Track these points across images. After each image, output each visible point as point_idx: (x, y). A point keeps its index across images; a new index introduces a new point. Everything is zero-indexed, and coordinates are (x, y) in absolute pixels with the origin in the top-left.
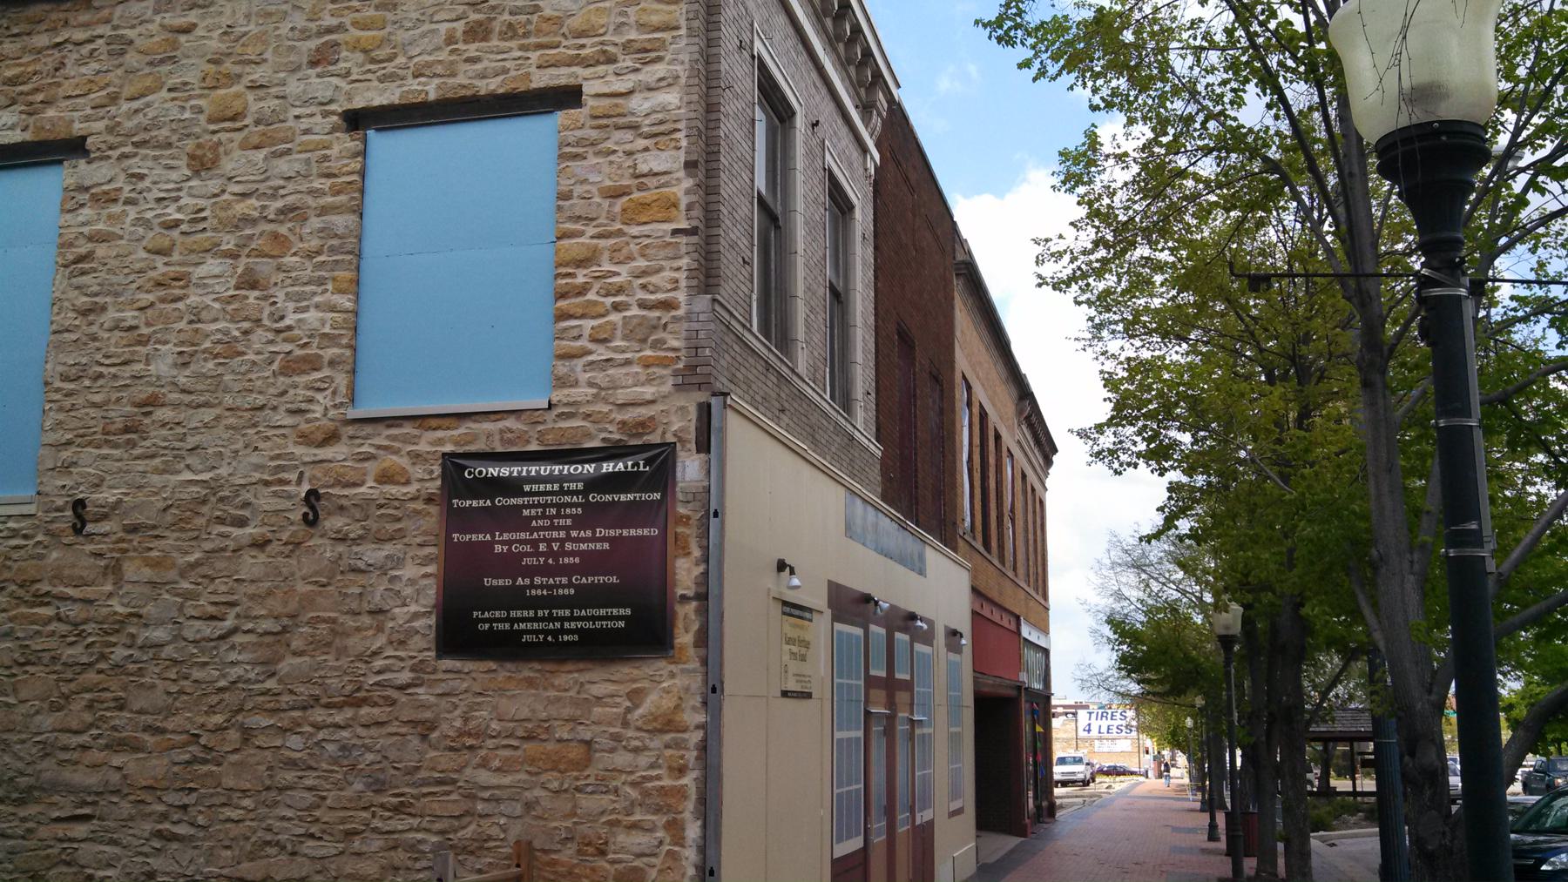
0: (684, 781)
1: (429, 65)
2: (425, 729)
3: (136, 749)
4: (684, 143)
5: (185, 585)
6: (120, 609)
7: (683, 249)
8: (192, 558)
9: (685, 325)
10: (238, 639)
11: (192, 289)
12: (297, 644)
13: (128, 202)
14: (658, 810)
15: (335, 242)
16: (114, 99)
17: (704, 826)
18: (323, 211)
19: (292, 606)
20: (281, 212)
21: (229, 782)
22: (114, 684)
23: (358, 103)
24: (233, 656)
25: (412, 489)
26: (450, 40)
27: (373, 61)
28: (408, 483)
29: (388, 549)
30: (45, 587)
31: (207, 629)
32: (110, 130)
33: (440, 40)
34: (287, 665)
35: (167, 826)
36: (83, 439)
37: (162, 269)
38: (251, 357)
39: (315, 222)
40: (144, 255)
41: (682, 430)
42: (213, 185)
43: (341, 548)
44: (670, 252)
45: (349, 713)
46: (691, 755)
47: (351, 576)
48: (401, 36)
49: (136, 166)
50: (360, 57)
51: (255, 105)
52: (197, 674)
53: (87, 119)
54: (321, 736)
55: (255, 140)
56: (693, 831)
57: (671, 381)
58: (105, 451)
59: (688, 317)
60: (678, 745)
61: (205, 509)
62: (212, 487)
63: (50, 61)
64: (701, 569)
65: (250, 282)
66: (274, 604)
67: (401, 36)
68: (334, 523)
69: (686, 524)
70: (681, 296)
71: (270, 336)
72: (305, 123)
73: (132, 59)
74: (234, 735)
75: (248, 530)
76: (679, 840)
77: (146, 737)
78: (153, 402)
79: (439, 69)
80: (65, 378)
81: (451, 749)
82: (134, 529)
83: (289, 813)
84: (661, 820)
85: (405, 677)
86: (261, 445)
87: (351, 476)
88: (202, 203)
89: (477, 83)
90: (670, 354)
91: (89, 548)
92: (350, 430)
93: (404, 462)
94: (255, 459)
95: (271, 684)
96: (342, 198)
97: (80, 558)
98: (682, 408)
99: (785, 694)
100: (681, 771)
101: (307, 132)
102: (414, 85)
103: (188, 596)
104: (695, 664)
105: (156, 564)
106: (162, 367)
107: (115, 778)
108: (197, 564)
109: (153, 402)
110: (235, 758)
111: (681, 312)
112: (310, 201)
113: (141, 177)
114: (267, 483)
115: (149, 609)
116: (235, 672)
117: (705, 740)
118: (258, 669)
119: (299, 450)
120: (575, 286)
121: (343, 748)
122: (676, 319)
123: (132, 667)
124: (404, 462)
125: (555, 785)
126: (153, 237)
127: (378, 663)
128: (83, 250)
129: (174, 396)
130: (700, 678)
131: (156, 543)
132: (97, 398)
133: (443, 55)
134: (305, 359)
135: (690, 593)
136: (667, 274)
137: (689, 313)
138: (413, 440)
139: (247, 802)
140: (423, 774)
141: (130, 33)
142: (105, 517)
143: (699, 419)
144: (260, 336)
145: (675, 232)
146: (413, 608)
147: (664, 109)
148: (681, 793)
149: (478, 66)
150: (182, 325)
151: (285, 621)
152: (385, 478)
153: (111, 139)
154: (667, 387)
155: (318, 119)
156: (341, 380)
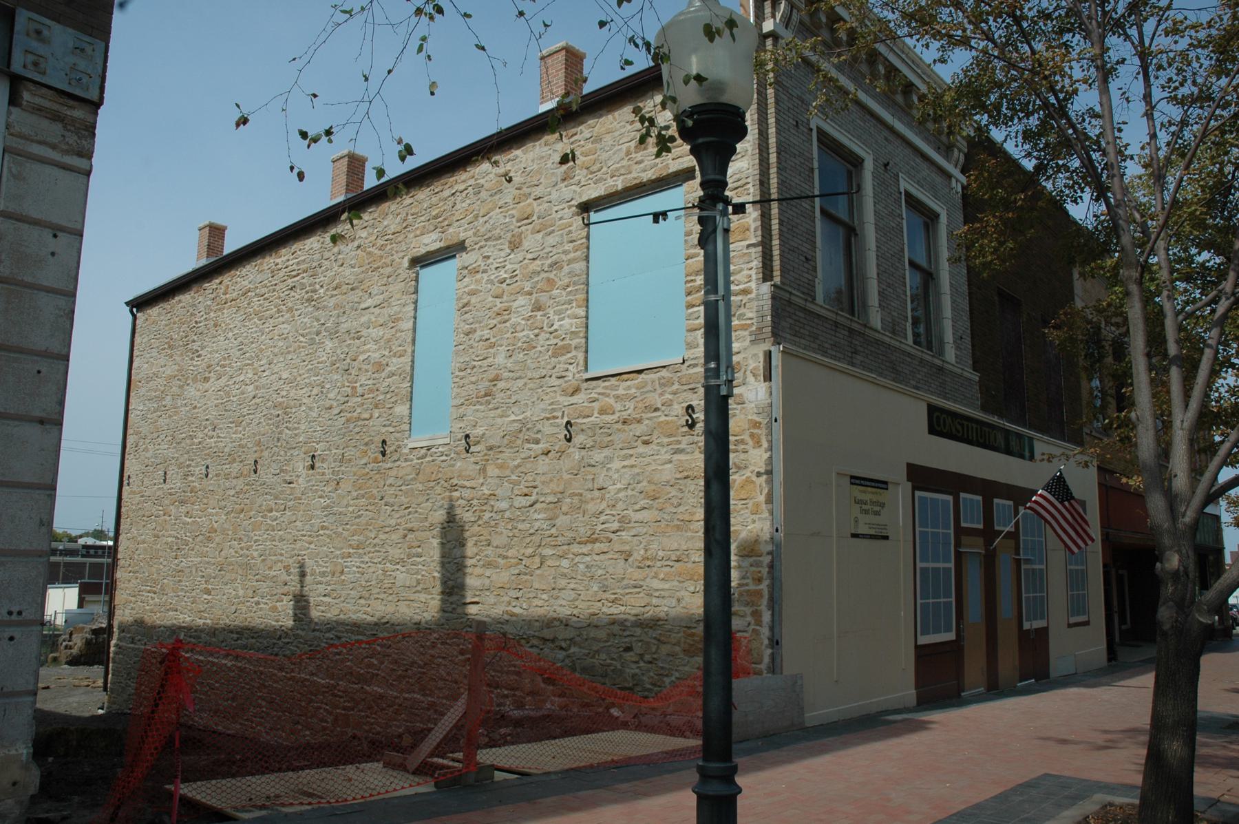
0: (761, 587)
1: (617, 169)
2: (627, 556)
3: (496, 567)
4: (752, 190)
5: (514, 477)
6: (487, 492)
7: (754, 256)
8: (516, 463)
9: (756, 303)
10: (538, 506)
11: (512, 315)
12: (564, 509)
13: (484, 272)
14: (747, 604)
15: (576, 279)
16: (476, 217)
17: (773, 615)
18: (570, 262)
19: (561, 488)
20: (551, 266)
21: (536, 585)
22: (485, 532)
23: (584, 198)
24: (536, 516)
25: (615, 417)
26: (628, 153)
27: (592, 173)
28: (613, 413)
29: (606, 452)
30: (455, 481)
31: (524, 501)
32: (475, 234)
33: (623, 154)
34: (562, 520)
35: (510, 608)
36: (468, 402)
37: (499, 305)
38: (539, 348)
39: (566, 269)
40: (491, 299)
41: (755, 368)
42: (520, 256)
43: (583, 452)
44: (746, 258)
45: (589, 546)
46: (765, 571)
47: (589, 469)
48: (604, 156)
49: (486, 251)
50: (585, 171)
51: (538, 208)
52: (520, 526)
53: (466, 230)
54: (577, 559)
55: (538, 228)
56: (766, 617)
57: (749, 339)
58: (478, 407)
59: (758, 298)
60: (758, 564)
61: (521, 435)
62: (523, 423)
63: (450, 203)
64: (768, 454)
65: (538, 307)
66: (553, 486)
67: (604, 156)
68: (578, 439)
69: (759, 428)
70: (753, 285)
71: (548, 335)
72: (560, 215)
73: (484, 195)
74: (537, 560)
75: (540, 446)
76: (759, 622)
77: (499, 560)
78: (497, 379)
79: (622, 171)
80: (461, 370)
81: (639, 567)
82: (490, 448)
83: (564, 603)
84: (748, 610)
85: (615, 526)
86: (545, 398)
87: (586, 412)
88: (516, 266)
89: (643, 175)
90: (749, 322)
91: (473, 459)
92: (585, 385)
93: (611, 401)
94: (542, 405)
95: (553, 531)
96: (579, 253)
97: (466, 466)
98: (755, 355)
99: (854, 536)
100: (760, 580)
101: (561, 219)
102: (610, 182)
103: (515, 483)
104: (766, 514)
105: (501, 467)
106: (500, 359)
107: (487, 582)
108: (519, 466)
109: (497, 379)
110: (538, 572)
111: (753, 295)
112: (564, 257)
113: (488, 257)
114: (548, 419)
115: (499, 492)
116: (537, 525)
117: (772, 561)
118: (548, 522)
119: (562, 399)
120: (694, 287)
121: (587, 567)
122: (751, 300)
123: (493, 523)
124: (611, 401)
125: (692, 589)
126: (495, 289)
127: (603, 518)
128: (465, 301)
129: (506, 374)
130: (769, 523)
131: (501, 455)
132: (473, 379)
133: (625, 163)
134: (563, 347)
135: (762, 470)
136: (746, 272)
137: (758, 295)
138: (615, 388)
139: (545, 597)
140: (625, 582)
141: (482, 181)
142: (478, 442)
143: (765, 361)
144: (543, 336)
145: (749, 246)
146: (619, 486)
147: (740, 172)
148: (759, 594)
149: (642, 165)
150: (509, 335)
151: (559, 496)
152: (602, 412)
153: (476, 239)
154: (747, 343)
155: (566, 210)
156: (581, 356)
